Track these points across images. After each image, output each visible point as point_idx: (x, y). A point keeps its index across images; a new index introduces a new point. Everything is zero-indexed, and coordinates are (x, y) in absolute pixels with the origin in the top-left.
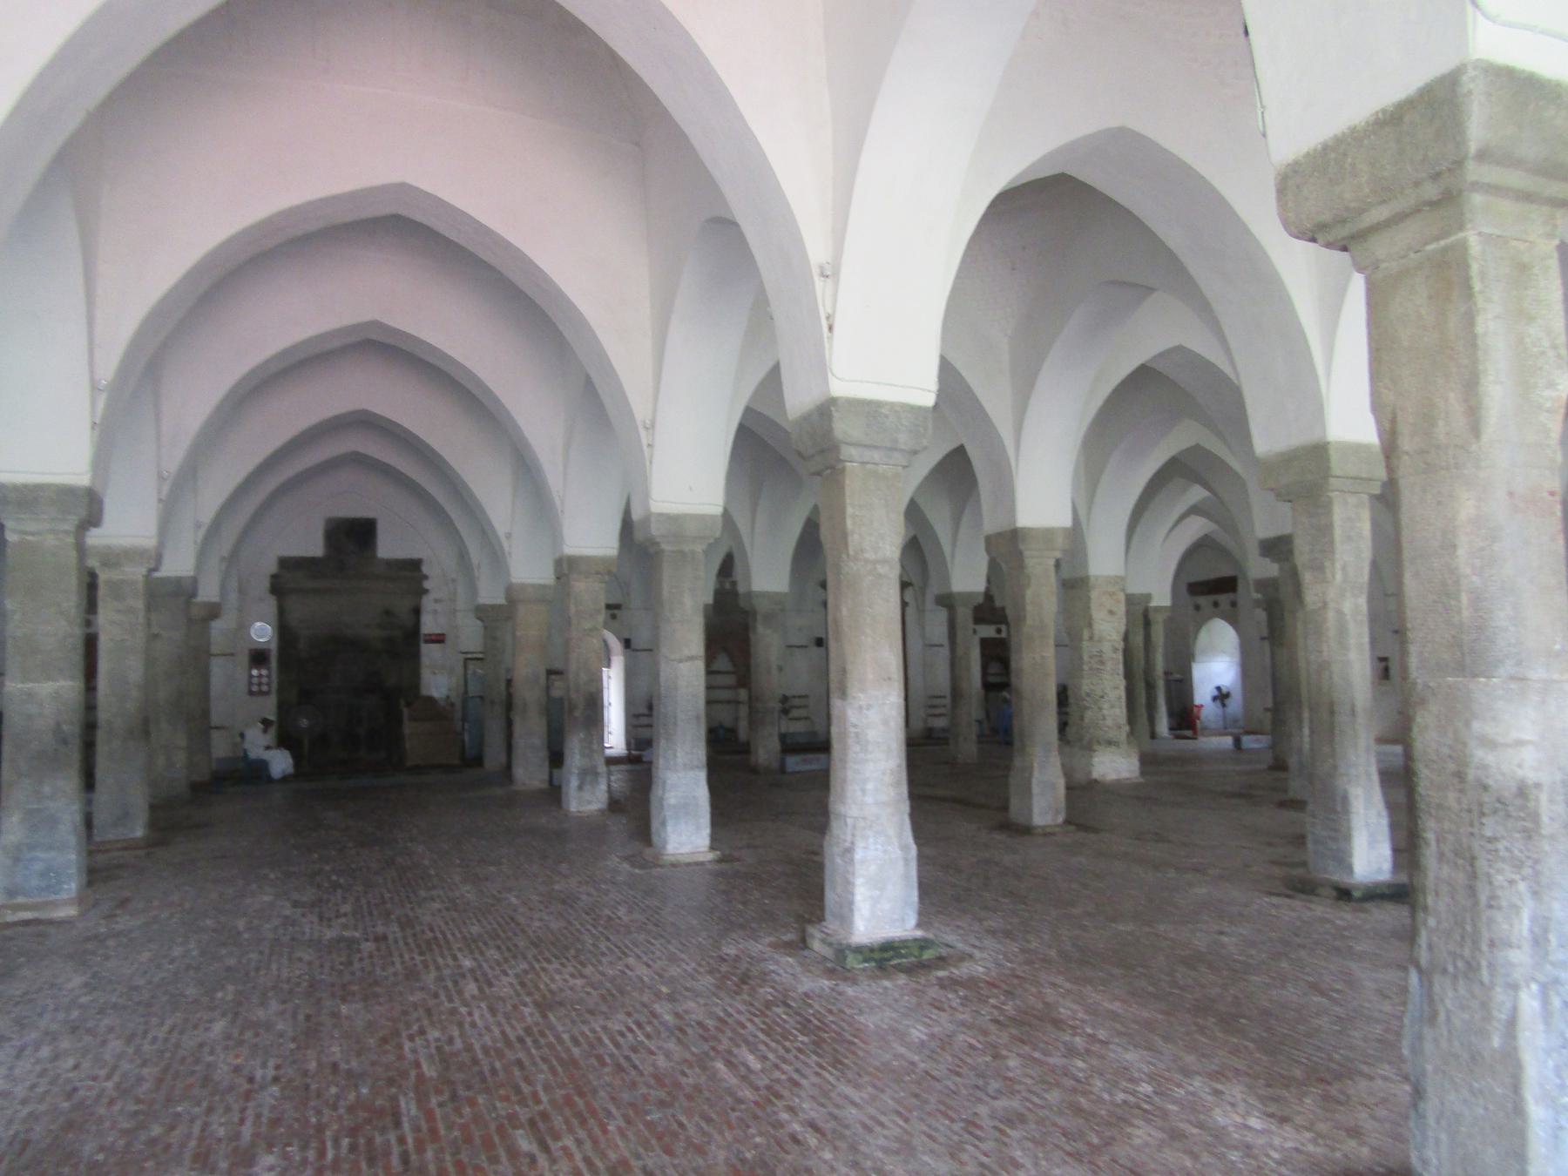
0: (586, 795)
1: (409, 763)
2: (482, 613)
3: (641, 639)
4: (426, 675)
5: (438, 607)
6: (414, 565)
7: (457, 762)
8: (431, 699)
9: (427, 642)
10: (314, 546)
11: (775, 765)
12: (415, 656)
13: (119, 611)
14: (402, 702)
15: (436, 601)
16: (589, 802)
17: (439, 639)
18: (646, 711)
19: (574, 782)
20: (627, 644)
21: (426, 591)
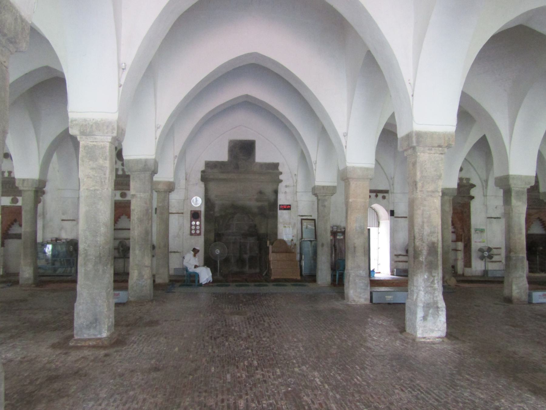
0: (429, 324)
1: (272, 278)
2: (316, 191)
3: (402, 209)
4: (280, 227)
5: (287, 190)
6: (275, 166)
7: (299, 278)
8: (283, 242)
9: (280, 209)
10: (223, 156)
11: (525, 298)
12: (275, 217)
13: (93, 169)
14: (268, 242)
15: (286, 186)
16: (432, 331)
17: (287, 208)
18: (404, 253)
19: (420, 314)
20: (392, 213)
21: (281, 181)
